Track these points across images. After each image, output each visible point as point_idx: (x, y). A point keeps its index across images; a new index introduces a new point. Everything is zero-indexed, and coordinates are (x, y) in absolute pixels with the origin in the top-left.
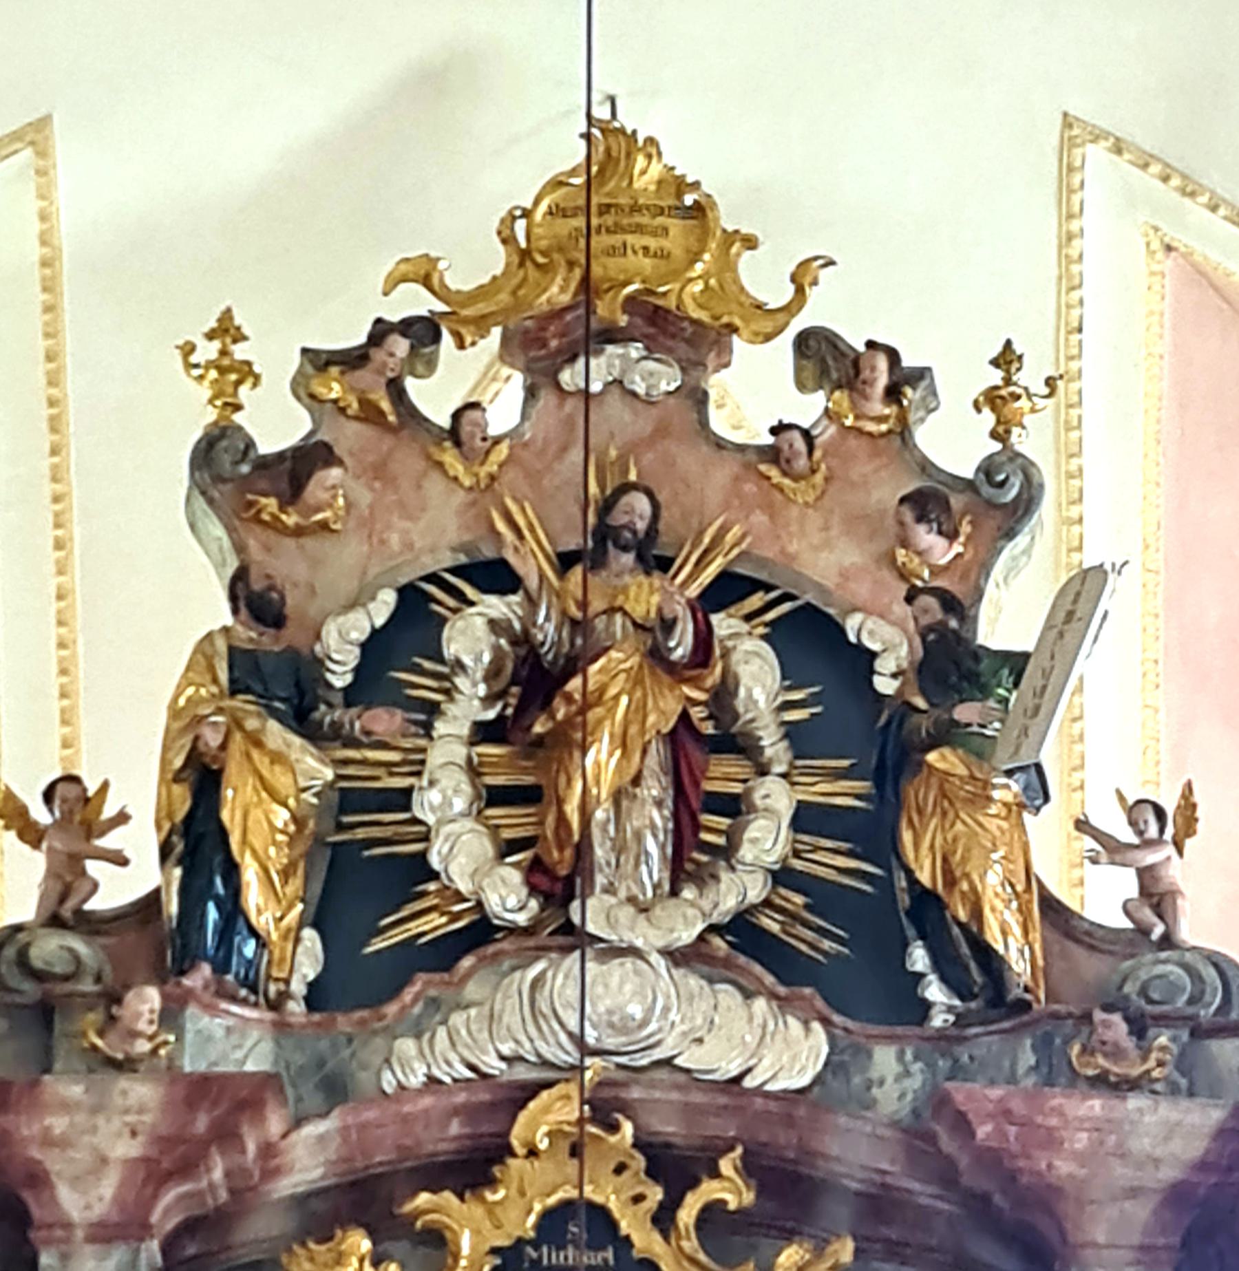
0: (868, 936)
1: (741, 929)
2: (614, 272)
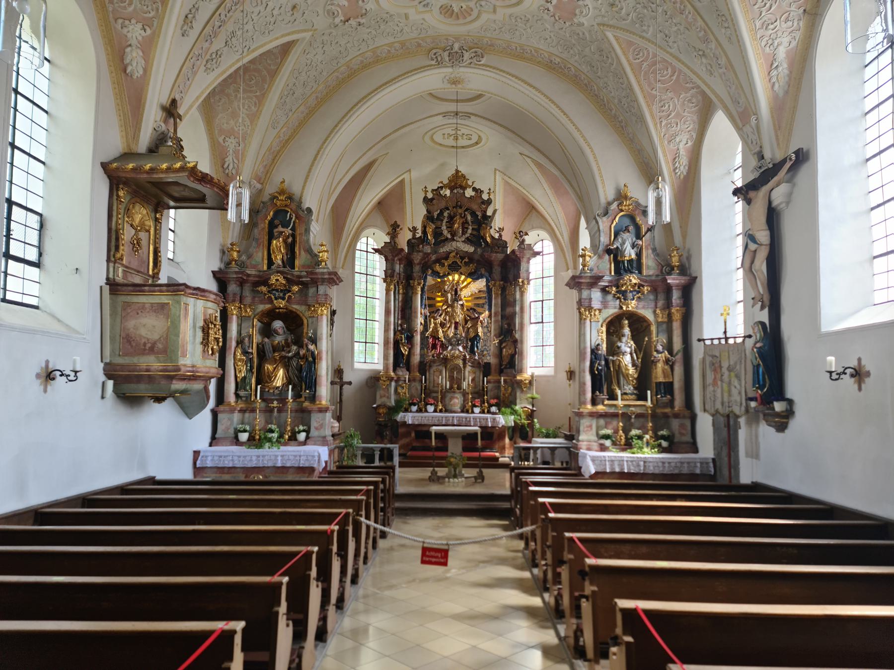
0: (477, 239)
1: (467, 238)
2: (458, 181)
